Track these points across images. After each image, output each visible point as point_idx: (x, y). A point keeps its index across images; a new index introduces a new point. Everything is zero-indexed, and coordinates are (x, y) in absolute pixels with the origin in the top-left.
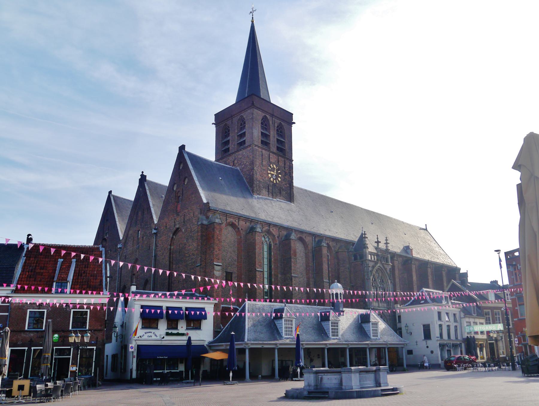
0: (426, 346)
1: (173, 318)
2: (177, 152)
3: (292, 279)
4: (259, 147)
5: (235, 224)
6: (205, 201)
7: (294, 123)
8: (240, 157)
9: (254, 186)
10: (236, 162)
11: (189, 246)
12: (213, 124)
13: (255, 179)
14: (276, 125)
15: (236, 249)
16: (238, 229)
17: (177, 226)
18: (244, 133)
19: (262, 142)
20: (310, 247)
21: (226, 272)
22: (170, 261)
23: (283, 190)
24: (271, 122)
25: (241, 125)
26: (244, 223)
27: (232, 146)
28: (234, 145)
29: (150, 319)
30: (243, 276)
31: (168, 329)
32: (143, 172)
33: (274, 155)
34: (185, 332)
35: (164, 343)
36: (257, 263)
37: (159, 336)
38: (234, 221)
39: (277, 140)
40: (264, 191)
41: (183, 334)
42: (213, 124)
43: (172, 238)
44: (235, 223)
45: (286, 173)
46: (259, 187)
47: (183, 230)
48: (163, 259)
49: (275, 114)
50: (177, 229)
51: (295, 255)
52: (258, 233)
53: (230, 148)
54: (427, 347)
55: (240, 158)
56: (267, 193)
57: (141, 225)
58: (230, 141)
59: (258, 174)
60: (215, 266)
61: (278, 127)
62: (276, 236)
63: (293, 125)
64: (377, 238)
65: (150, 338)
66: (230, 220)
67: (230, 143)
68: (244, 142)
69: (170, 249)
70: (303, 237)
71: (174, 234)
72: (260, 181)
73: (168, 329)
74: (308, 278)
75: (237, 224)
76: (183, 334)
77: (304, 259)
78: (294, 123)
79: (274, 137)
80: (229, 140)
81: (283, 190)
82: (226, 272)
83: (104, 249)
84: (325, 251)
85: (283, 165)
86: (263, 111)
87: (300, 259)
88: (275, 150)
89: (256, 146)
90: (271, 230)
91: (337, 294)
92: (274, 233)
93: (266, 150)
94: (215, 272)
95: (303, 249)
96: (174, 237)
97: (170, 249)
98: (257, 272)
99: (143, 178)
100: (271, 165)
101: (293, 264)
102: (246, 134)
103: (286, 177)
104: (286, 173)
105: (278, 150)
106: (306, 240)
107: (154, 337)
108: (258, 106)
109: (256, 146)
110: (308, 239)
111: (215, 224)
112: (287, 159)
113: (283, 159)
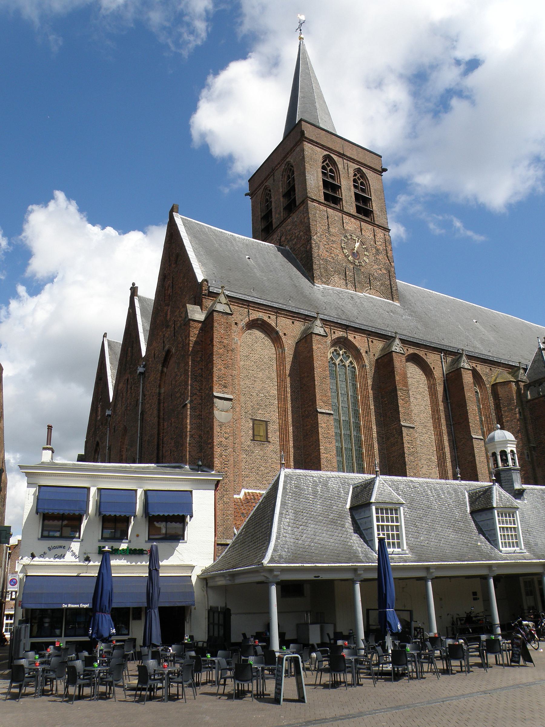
3: (401, 433)
4: (320, 203)
5: (269, 325)
6: (200, 278)
8: (289, 227)
9: (315, 267)
10: (283, 239)
12: (246, 195)
13: (315, 255)
14: (351, 172)
15: (274, 375)
16: (277, 333)
17: (167, 347)
19: (327, 197)
20: (438, 374)
21: (254, 420)
22: (159, 417)
24: (340, 166)
25: (289, 177)
26: (289, 322)
28: (279, 214)
31: (104, 539)
33: (353, 219)
34: (146, 547)
36: (318, 397)
38: (266, 318)
39: (356, 194)
42: (246, 195)
43: (162, 372)
44: (268, 321)
46: (326, 270)
50: (168, 352)
51: (406, 384)
52: (318, 337)
55: (290, 231)
56: (343, 282)
58: (273, 210)
59: (322, 247)
60: (216, 400)
61: (355, 175)
62: (363, 351)
63: (384, 174)
66: (256, 315)
69: (160, 394)
70: (421, 353)
71: (163, 366)
72: (326, 261)
73: (104, 539)
74: (439, 435)
75: (273, 324)
77: (427, 398)
78: (385, 170)
79: (350, 190)
80: (271, 210)
82: (254, 420)
84: (468, 378)
85: (372, 236)
86: (323, 147)
87: (418, 396)
88: (353, 211)
89: (313, 200)
90: (349, 338)
92: (357, 344)
93: (334, 208)
95: (423, 377)
96: (165, 370)
97: (160, 394)
98: (320, 416)
100: (348, 235)
101: (400, 402)
103: (380, 257)
104: (377, 250)
105: (358, 212)
106: (428, 361)
108: (314, 138)
109: (313, 200)
110: (432, 359)
112: (379, 226)
113: (370, 227)
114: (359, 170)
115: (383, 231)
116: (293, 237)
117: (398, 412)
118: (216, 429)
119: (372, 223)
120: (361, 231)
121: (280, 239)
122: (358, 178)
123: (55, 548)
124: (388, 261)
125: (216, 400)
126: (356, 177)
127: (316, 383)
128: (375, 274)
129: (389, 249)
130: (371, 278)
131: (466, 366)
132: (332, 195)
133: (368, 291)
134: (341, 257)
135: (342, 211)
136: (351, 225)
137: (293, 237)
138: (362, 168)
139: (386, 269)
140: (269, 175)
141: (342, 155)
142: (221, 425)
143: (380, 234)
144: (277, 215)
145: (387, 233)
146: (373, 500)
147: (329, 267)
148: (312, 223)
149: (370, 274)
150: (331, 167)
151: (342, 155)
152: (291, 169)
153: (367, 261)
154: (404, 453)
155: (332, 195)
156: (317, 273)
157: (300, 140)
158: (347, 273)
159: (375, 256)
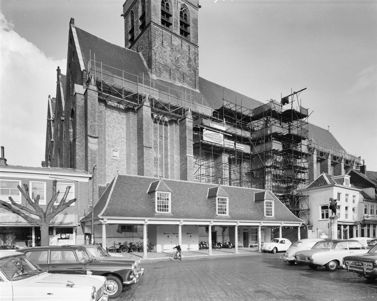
7: (200, 7)
10: (139, 47)
15: (124, 127)
23: (187, 76)
27: (138, 32)
32: (58, 67)
46: (159, 69)
61: (182, 9)
63: (199, 9)
78: (200, 7)
81: (187, 76)
88: (178, 33)
94: (89, 145)
104: (190, 59)
113: (187, 44)
114: (184, 5)
115: (195, 47)
119: (189, 41)
120: (182, 46)
121: (137, 47)
122: (183, 11)
124: (195, 66)
125: (89, 138)
126: (182, 10)
127: (144, 132)
128: (187, 73)
129: (196, 59)
130: (185, 75)
132: (166, 23)
133: (182, 83)
135: (171, 32)
136: (177, 42)
138: (186, 4)
139: (194, 71)
142: (91, 151)
143: (192, 49)
145: (196, 49)
146: (156, 190)
147: (161, 67)
149: (184, 73)
150: (167, 2)
153: (183, 64)
155: (166, 23)
158: (171, 71)
159: (188, 63)
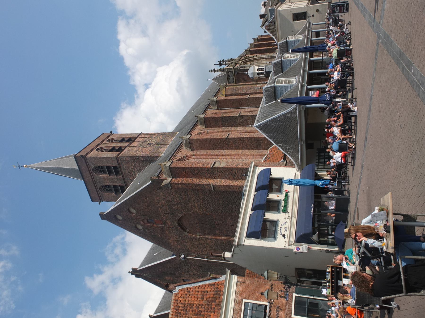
0: (312, 17)
1: (265, 206)
2: (106, 222)
3: (242, 116)
7: (111, 132)
9: (153, 156)
11: (195, 206)
17: (176, 224)
18: (107, 167)
24: (104, 146)
29: (265, 230)
30: (232, 153)
35: (295, 214)
37: (286, 222)
40: (160, 150)
41: (287, 196)
43: (188, 232)
44: (178, 159)
45: (150, 137)
47: (180, 215)
48: (210, 247)
49: (98, 143)
50: (179, 224)
53: (120, 184)
54: (313, 16)
57: (178, 277)
64: (217, 64)
65: (288, 229)
67: (116, 184)
68: (115, 168)
71: (185, 231)
72: (151, 152)
76: (287, 196)
78: (111, 132)
80: (113, 186)
83: (177, 288)
85: (143, 139)
91: (258, 70)
94: (220, 167)
99: (136, 272)
102: (108, 165)
104: (150, 137)
107: (287, 226)
111: (171, 166)
116: (133, 170)
117: (232, 117)
118: (229, 166)
123: (281, 231)
125: (215, 166)
131: (216, 98)
134: (150, 148)
137: (133, 170)
140: (95, 185)
141: (98, 145)
144: (118, 182)
148: (130, 155)
151: (98, 145)
152: (97, 169)
154: (251, 115)
156: (156, 155)
157: (84, 159)
